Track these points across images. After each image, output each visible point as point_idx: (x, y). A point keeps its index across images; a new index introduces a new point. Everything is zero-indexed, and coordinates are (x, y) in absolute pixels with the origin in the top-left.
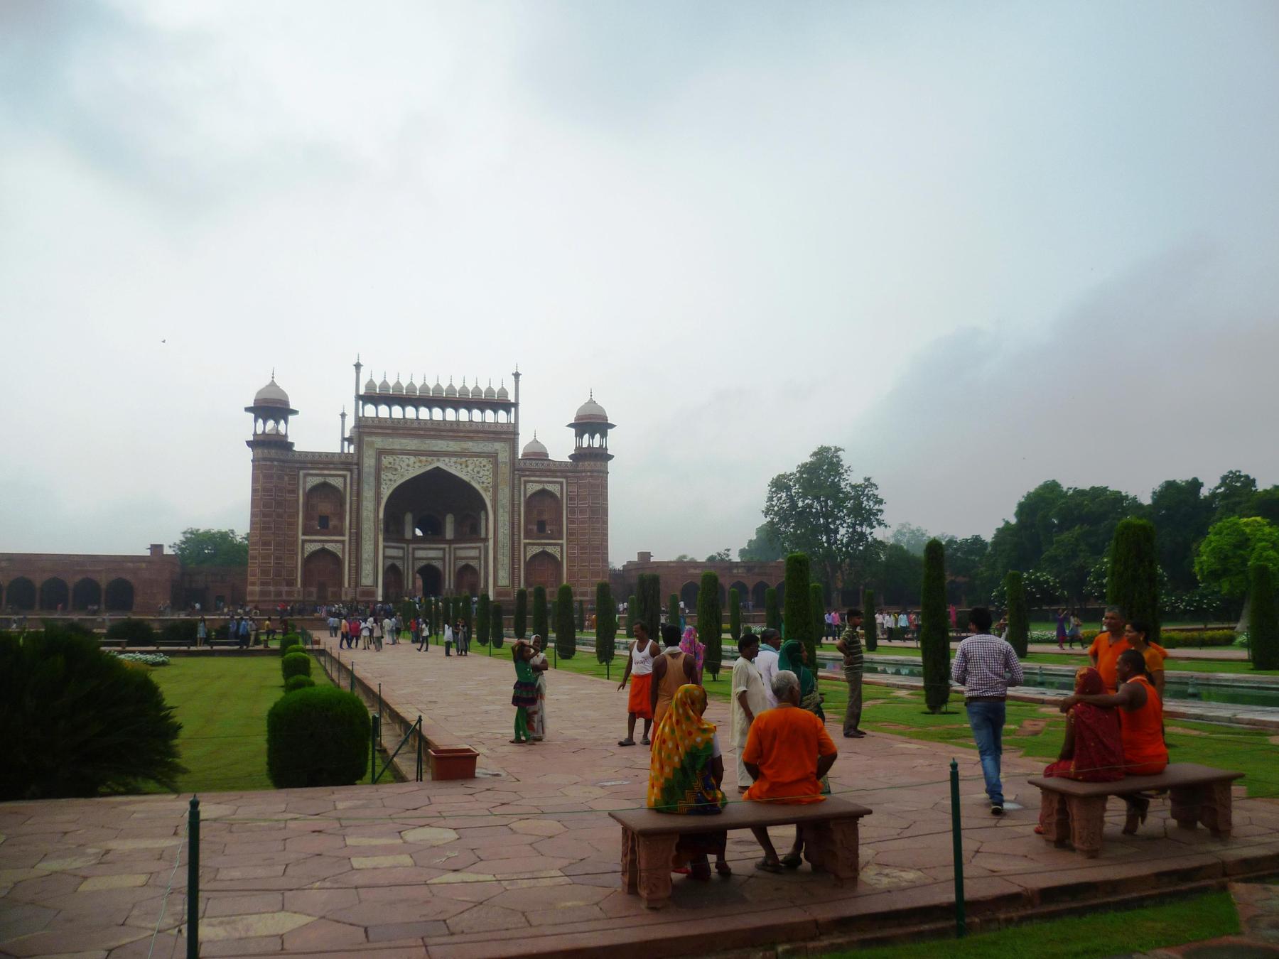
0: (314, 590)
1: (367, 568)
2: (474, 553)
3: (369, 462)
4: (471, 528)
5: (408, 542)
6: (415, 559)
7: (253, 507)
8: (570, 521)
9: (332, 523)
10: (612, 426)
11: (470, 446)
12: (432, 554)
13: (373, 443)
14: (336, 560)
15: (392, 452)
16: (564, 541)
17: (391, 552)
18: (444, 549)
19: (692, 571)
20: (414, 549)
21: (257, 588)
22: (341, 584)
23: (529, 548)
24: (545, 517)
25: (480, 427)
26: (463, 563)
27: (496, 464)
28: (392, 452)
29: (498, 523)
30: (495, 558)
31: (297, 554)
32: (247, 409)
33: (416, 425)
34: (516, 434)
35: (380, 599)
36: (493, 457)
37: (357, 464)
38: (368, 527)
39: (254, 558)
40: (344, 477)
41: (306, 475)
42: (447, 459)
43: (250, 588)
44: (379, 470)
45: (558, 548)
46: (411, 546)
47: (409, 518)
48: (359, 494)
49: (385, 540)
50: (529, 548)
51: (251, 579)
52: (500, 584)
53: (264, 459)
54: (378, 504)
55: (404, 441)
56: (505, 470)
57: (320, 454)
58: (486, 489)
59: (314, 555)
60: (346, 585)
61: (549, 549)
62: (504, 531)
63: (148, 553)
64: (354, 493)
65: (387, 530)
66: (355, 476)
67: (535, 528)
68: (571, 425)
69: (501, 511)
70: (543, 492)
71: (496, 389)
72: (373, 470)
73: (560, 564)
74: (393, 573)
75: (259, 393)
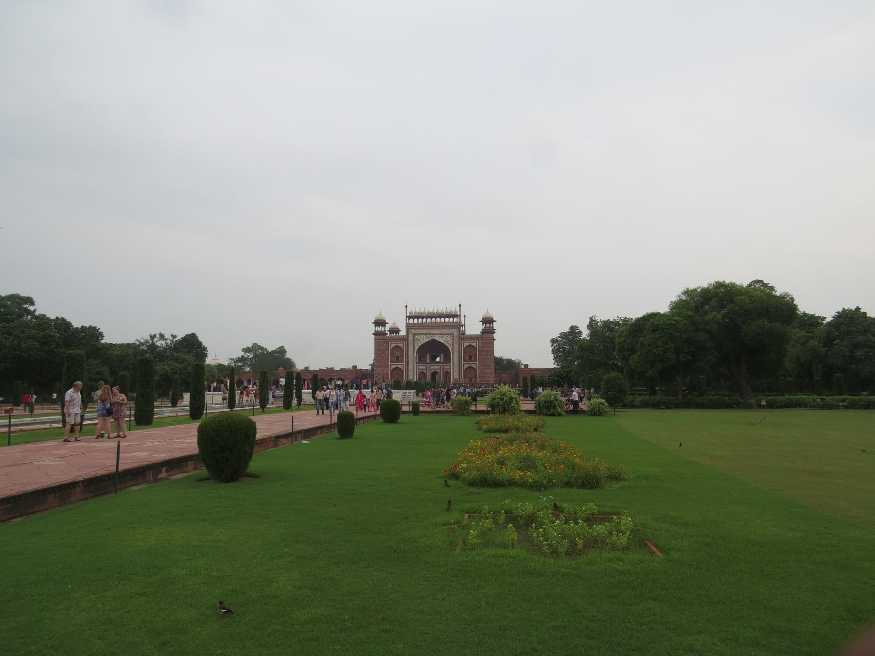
1: (411, 373)
3: (411, 338)
11: (444, 331)
14: (402, 371)
15: (418, 335)
27: (453, 336)
28: (418, 335)
29: (455, 358)
36: (452, 334)
38: (411, 359)
44: (414, 340)
47: (428, 355)
56: (456, 339)
62: (456, 359)
65: (420, 359)
74: (422, 374)
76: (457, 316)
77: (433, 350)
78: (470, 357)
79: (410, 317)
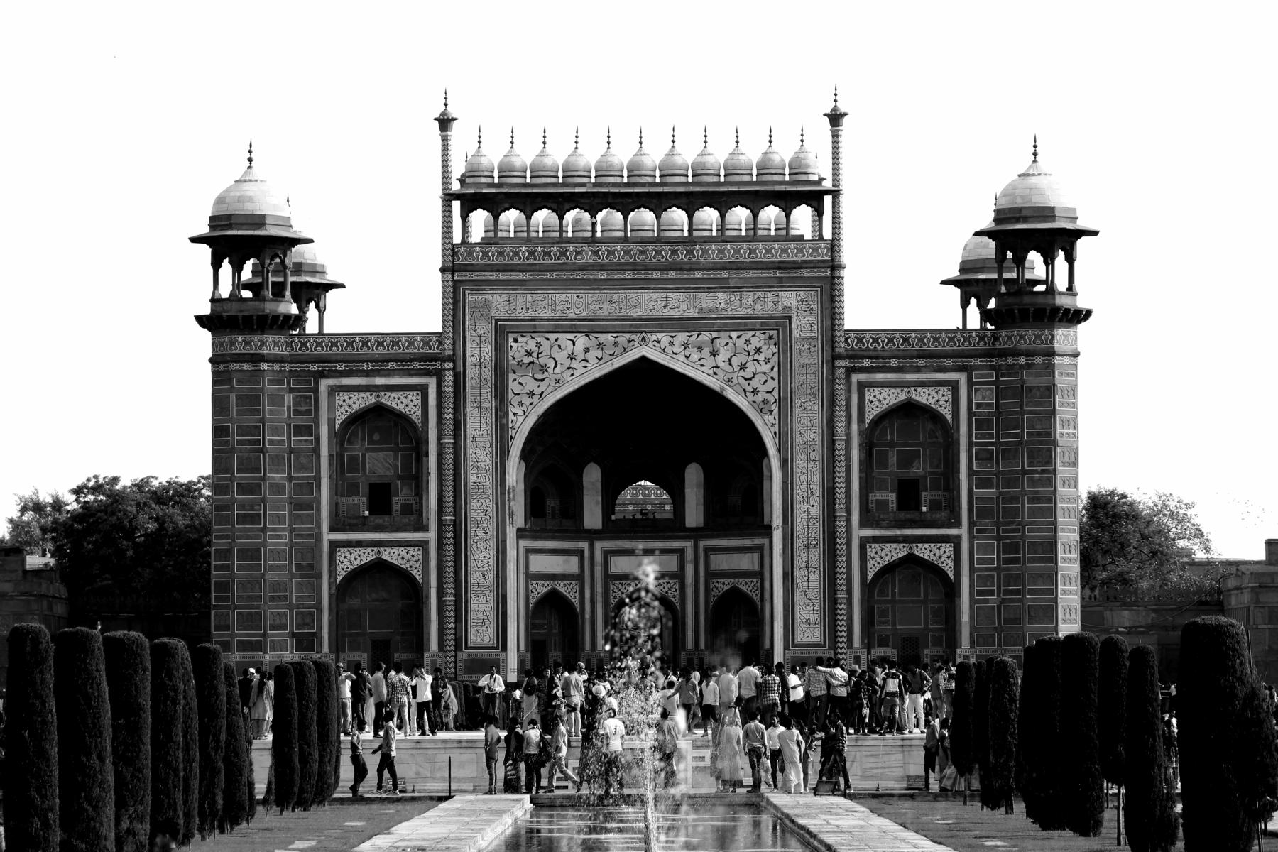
1: (481, 605)
2: (746, 562)
3: (478, 353)
4: (738, 501)
5: (592, 535)
6: (608, 577)
8: (979, 481)
9: (397, 501)
11: (722, 302)
13: (487, 304)
15: (532, 327)
16: (963, 532)
17: (541, 564)
18: (681, 552)
20: (607, 554)
23: (872, 549)
24: (919, 469)
26: (724, 585)
28: (532, 327)
29: (795, 490)
30: (788, 576)
31: (318, 576)
32: (193, 240)
34: (835, 266)
36: (779, 327)
37: (452, 359)
38: (479, 506)
41: (333, 391)
42: (665, 338)
45: (948, 549)
46: (600, 546)
47: (592, 476)
49: (521, 534)
50: (872, 549)
52: (800, 639)
53: (239, 358)
54: (502, 453)
55: (560, 297)
56: (808, 360)
57: (365, 338)
58: (763, 409)
60: (434, 646)
62: (808, 509)
64: (449, 427)
66: (449, 389)
67: (892, 497)
69: (800, 461)
71: (784, 153)
72: (488, 373)
73: (951, 589)
75: (220, 201)
76: (814, 198)
77: (646, 436)
78: (908, 493)
79: (471, 202)
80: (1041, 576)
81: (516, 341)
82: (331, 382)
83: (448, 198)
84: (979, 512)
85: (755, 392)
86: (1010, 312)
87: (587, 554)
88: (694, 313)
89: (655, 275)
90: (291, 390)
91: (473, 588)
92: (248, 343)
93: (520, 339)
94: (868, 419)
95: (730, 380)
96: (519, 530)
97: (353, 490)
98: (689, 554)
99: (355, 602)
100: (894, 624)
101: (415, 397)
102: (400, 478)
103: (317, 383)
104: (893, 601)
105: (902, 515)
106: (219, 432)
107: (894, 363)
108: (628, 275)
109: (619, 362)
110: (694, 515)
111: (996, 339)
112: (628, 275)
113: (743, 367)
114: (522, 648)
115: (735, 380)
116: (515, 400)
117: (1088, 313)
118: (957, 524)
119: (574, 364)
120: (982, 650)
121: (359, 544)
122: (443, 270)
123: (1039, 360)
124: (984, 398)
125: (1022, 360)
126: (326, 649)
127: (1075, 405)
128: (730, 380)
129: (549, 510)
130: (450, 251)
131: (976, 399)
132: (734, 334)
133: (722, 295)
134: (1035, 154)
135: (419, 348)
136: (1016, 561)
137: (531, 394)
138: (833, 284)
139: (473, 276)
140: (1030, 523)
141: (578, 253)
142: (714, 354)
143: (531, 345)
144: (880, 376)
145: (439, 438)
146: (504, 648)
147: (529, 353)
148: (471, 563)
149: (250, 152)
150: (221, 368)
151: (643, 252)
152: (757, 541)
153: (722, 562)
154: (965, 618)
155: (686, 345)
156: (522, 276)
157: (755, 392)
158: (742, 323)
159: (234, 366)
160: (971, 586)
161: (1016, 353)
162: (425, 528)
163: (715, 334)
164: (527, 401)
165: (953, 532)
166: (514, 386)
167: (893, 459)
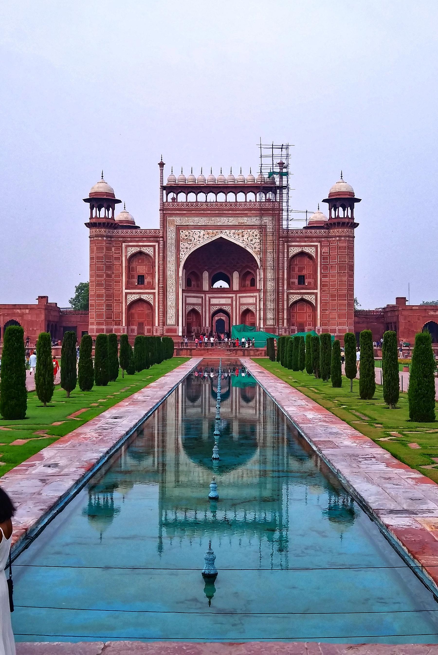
0: (135, 328)
1: (171, 312)
3: (171, 235)
4: (249, 283)
5: (205, 292)
6: (210, 305)
7: (91, 270)
8: (323, 276)
10: (358, 200)
12: (223, 301)
15: (187, 227)
16: (318, 291)
18: (232, 297)
19: (432, 313)
20: (210, 298)
21: (95, 327)
22: (153, 324)
23: (291, 296)
24: (305, 272)
25: (252, 206)
26: (244, 308)
28: (187, 227)
31: (122, 303)
33: (205, 207)
35: (180, 334)
37: (163, 237)
39: (92, 306)
40: (154, 246)
41: (127, 247)
42: (228, 232)
43: (90, 327)
44: (178, 241)
45: (313, 297)
46: (208, 296)
47: (206, 275)
48: (164, 258)
50: (291, 296)
51: (91, 320)
53: (97, 236)
59: (134, 303)
60: (157, 325)
61: (306, 297)
63: (36, 302)
64: (161, 258)
65: (188, 283)
66: (161, 246)
67: (296, 281)
68: (324, 201)
70: (302, 254)
72: (174, 242)
73: (314, 308)
78: (301, 279)
80: (343, 304)
81: (182, 232)
82: (126, 244)
83: (163, 188)
84: (322, 285)
85: (255, 248)
86: (335, 223)
87: (204, 298)
88: (237, 224)
89: (225, 212)
90: (114, 246)
91: (168, 307)
92: (100, 231)
93: (184, 231)
94: (290, 256)
95: (248, 244)
96: (182, 290)
97: (133, 277)
98: (234, 298)
99: (133, 311)
100: (296, 319)
101: (152, 249)
102: (147, 273)
103: (122, 244)
104: (296, 312)
105: (300, 286)
106: (92, 258)
107: (298, 239)
108: (217, 212)
109: (214, 239)
110: (236, 287)
111: (329, 232)
112: (217, 212)
113: (252, 240)
114: (184, 325)
115: (249, 245)
116: (182, 250)
117: (358, 224)
118: (317, 289)
119: (200, 239)
120: (324, 327)
121: (134, 293)
122: (160, 210)
123: (343, 238)
124: (325, 250)
125: (338, 238)
126: (124, 325)
127: (353, 253)
128: (248, 244)
129: (192, 285)
130: (163, 204)
131: (323, 250)
132: (249, 230)
133: (246, 219)
134: (342, 177)
135: (153, 234)
136: (335, 300)
137: (187, 248)
138: (279, 216)
139: (169, 212)
140: (339, 288)
141: (202, 205)
142: (243, 236)
143: (187, 233)
144: (293, 244)
145: (159, 262)
146: (178, 325)
147: (186, 236)
148: (168, 299)
149: (102, 174)
150: (92, 239)
151: (221, 205)
152: (255, 294)
153: (244, 301)
154: (319, 317)
155: (234, 233)
156: (184, 212)
157: (255, 248)
158: (251, 227)
159: (95, 238)
160: (321, 308)
161: (335, 237)
162: (154, 289)
163: (243, 230)
164: (185, 250)
165: (315, 291)
166: (181, 246)
167: (297, 269)
